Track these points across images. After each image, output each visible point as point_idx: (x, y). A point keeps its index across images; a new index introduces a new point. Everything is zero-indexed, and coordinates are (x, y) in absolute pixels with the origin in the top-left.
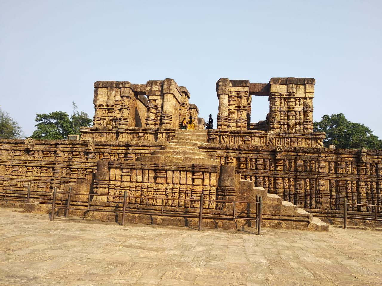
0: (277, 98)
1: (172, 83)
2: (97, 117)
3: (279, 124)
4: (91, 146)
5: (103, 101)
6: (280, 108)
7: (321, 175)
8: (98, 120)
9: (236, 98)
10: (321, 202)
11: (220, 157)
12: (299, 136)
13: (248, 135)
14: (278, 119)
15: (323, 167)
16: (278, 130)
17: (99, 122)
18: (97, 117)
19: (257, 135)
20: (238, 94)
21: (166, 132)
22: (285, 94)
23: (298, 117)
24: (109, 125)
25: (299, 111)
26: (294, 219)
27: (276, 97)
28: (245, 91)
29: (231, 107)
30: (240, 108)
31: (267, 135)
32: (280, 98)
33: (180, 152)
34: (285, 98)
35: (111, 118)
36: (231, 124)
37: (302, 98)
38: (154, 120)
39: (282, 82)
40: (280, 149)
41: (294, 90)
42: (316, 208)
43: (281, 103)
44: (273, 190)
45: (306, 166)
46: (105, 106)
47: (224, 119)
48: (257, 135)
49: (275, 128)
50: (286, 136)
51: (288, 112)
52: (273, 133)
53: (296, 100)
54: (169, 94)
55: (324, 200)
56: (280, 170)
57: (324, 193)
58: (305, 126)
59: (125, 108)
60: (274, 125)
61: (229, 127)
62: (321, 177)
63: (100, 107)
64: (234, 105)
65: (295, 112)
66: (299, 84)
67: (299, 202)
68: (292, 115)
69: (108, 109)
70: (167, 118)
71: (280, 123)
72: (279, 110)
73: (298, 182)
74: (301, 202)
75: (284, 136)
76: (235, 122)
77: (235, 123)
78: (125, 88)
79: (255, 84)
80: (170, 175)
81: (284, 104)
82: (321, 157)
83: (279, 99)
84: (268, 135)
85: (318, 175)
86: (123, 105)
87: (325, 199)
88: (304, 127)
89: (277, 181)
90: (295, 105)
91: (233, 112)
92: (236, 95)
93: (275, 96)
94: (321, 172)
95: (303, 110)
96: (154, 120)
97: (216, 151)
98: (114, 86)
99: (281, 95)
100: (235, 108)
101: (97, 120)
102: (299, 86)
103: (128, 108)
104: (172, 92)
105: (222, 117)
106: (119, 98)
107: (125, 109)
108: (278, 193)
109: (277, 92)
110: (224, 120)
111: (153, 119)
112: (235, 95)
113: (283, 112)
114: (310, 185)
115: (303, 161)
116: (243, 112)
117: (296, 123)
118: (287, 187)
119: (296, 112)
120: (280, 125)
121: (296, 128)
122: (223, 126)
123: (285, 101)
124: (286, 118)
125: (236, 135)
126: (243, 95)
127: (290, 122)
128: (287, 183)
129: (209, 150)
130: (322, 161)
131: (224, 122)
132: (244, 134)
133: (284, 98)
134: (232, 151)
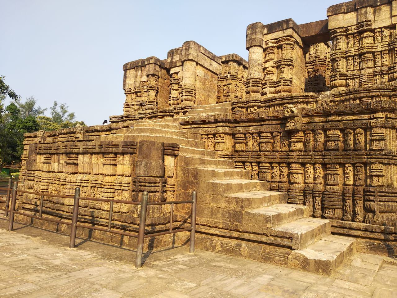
0: (341, 36)
1: (191, 46)
3: (345, 79)
5: (131, 84)
6: (346, 52)
7: (374, 156)
8: (127, 107)
9: (276, 50)
10: (373, 209)
11: (207, 135)
12: (374, 94)
13: (286, 101)
14: (344, 71)
15: (379, 140)
16: (343, 89)
19: (301, 100)
20: (277, 42)
21: (183, 111)
22: (353, 27)
23: (380, 62)
25: (381, 52)
26: (264, 239)
27: (338, 36)
28: (287, 36)
29: (268, 65)
30: (279, 63)
31: (317, 99)
32: (347, 36)
33: (135, 129)
34: (355, 33)
35: (138, 103)
37: (386, 28)
38: (176, 99)
39: (347, 9)
40: (292, 112)
41: (370, 16)
42: (363, 222)
43: (348, 43)
44: (285, 185)
45: (345, 142)
47: (253, 83)
48: (301, 100)
49: (337, 87)
50: (351, 96)
51: (360, 55)
52: (329, 94)
53: (375, 33)
54: (188, 62)
55: (380, 205)
56: (295, 149)
57: (380, 192)
58: (392, 74)
59: (150, 88)
60: (335, 81)
61: (263, 94)
62: (374, 160)
63: (128, 92)
64: (272, 60)
65: (373, 53)
66: (379, 4)
67: (329, 208)
68: (367, 60)
69: (136, 93)
70: (186, 93)
71: (346, 76)
72: (345, 56)
73: (330, 170)
74: (334, 209)
75: (347, 97)
76: (272, 86)
77: (272, 87)
78: (150, 65)
79: (309, 23)
80: (80, 161)
81: (354, 44)
82: (375, 120)
83: (344, 37)
84: (320, 98)
85: (369, 157)
86: (183, 90)
87: (381, 203)
88: (390, 77)
89: (292, 170)
90: (373, 42)
91: (270, 71)
92: (275, 45)
93: (335, 35)
94: (374, 149)
95: (387, 48)
96: (176, 99)
97: (201, 126)
98: (140, 64)
99: (347, 29)
102: (380, 9)
103: (155, 89)
104: (190, 57)
105: (251, 81)
106: (145, 78)
107: (150, 90)
108: (292, 191)
109: (339, 27)
110: (253, 85)
112: (273, 45)
113: (350, 58)
114: (354, 175)
115: (339, 131)
116: (286, 69)
117: (374, 72)
118: (311, 180)
119: (376, 54)
120: (346, 80)
121: (375, 82)
122: (251, 93)
123: (355, 39)
124: (357, 67)
125: (270, 104)
126: (284, 42)
127: (363, 72)
128: (309, 174)
129: (193, 126)
130: (376, 127)
131: (254, 87)
132: (280, 102)
133: (353, 34)
134: (221, 124)
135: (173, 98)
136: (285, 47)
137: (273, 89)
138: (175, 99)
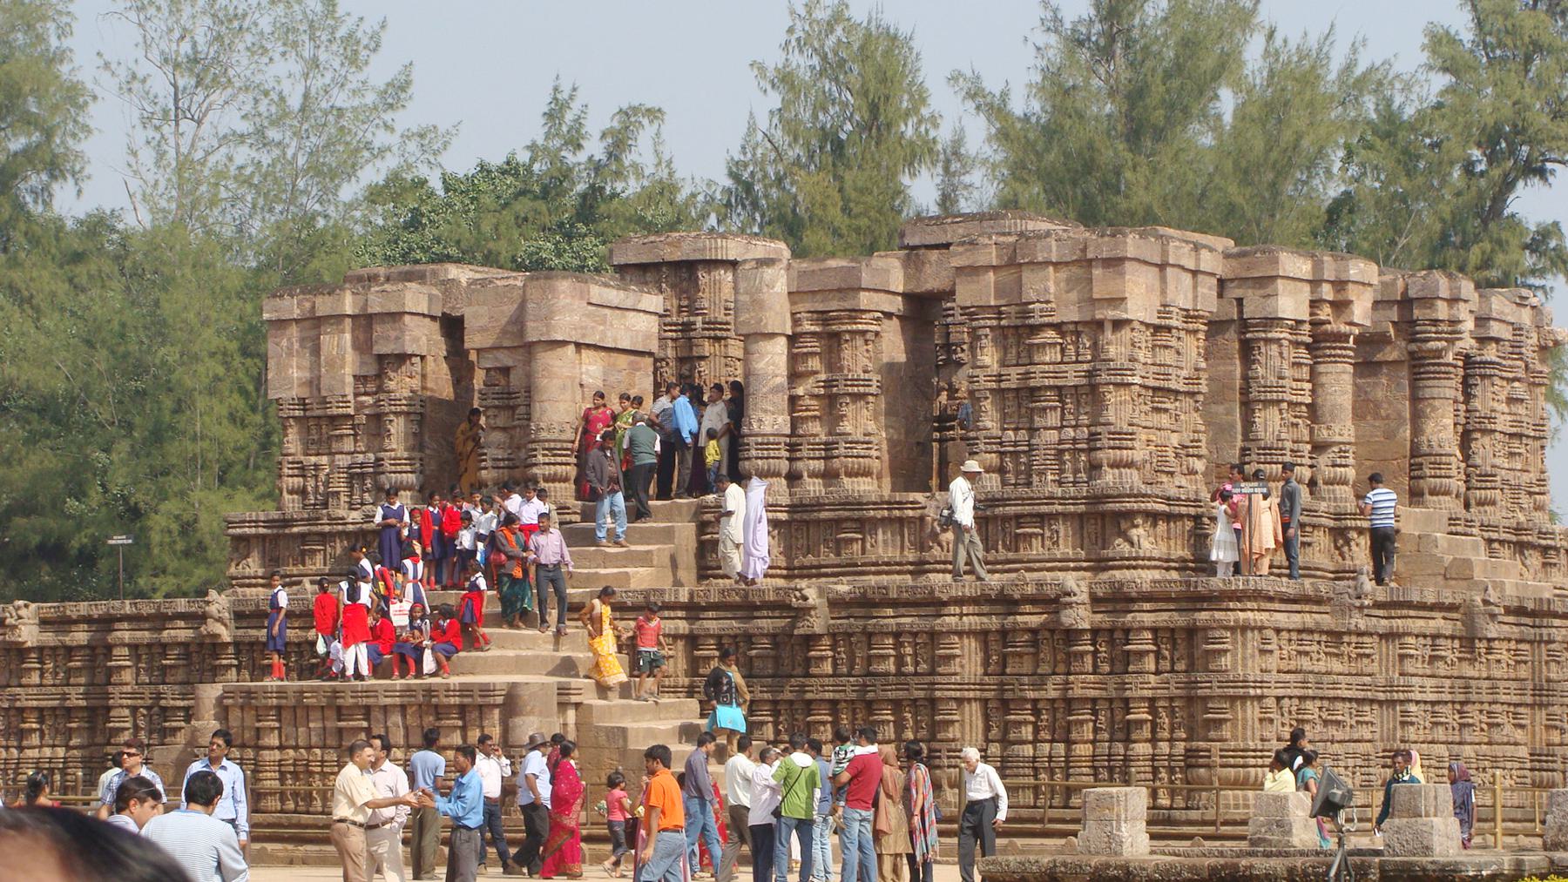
2: (290, 459)
4: (220, 620)
13: (847, 514)
17: (298, 481)
18: (290, 459)
24: (338, 493)
25: (1076, 387)
31: (926, 511)
36: (800, 465)
46: (315, 406)
65: (1059, 388)
70: (544, 455)
100: (816, 391)
101: (290, 472)
111: (503, 460)
112: (813, 328)
113: (1010, 395)
135: (494, 460)
136: (847, 341)
137: (819, 465)
138: (502, 464)
